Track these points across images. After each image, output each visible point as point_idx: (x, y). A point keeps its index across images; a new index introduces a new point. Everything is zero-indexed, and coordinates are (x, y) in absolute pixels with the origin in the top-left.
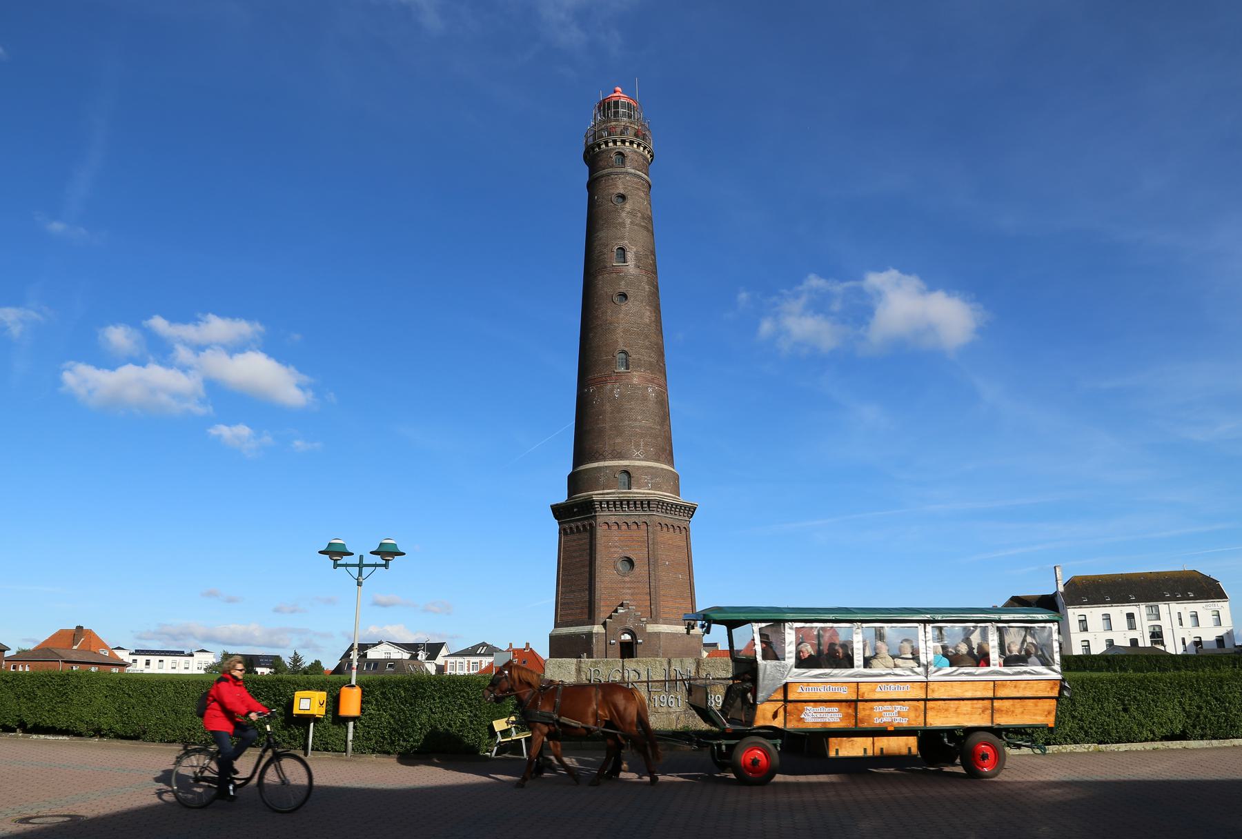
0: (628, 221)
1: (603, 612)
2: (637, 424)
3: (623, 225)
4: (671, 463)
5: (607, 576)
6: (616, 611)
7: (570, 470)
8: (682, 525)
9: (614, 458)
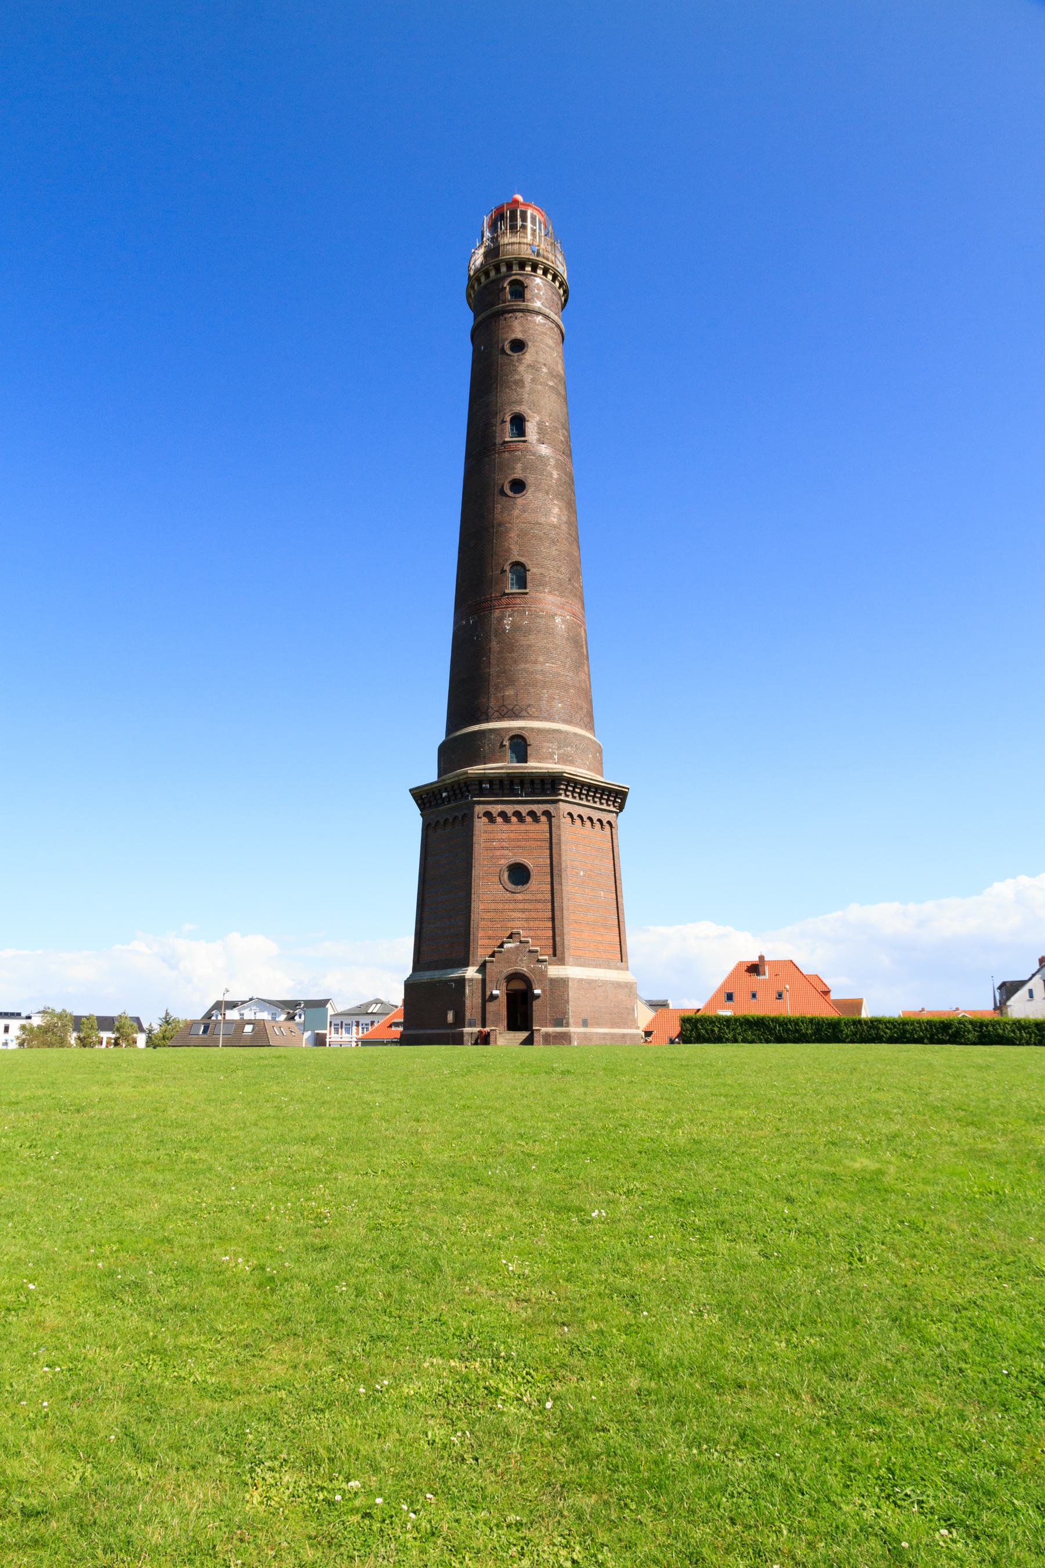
0: (528, 378)
1: (481, 950)
2: (539, 667)
3: (520, 383)
4: (590, 726)
5: (488, 891)
6: (501, 946)
8: (606, 817)
9: (502, 717)
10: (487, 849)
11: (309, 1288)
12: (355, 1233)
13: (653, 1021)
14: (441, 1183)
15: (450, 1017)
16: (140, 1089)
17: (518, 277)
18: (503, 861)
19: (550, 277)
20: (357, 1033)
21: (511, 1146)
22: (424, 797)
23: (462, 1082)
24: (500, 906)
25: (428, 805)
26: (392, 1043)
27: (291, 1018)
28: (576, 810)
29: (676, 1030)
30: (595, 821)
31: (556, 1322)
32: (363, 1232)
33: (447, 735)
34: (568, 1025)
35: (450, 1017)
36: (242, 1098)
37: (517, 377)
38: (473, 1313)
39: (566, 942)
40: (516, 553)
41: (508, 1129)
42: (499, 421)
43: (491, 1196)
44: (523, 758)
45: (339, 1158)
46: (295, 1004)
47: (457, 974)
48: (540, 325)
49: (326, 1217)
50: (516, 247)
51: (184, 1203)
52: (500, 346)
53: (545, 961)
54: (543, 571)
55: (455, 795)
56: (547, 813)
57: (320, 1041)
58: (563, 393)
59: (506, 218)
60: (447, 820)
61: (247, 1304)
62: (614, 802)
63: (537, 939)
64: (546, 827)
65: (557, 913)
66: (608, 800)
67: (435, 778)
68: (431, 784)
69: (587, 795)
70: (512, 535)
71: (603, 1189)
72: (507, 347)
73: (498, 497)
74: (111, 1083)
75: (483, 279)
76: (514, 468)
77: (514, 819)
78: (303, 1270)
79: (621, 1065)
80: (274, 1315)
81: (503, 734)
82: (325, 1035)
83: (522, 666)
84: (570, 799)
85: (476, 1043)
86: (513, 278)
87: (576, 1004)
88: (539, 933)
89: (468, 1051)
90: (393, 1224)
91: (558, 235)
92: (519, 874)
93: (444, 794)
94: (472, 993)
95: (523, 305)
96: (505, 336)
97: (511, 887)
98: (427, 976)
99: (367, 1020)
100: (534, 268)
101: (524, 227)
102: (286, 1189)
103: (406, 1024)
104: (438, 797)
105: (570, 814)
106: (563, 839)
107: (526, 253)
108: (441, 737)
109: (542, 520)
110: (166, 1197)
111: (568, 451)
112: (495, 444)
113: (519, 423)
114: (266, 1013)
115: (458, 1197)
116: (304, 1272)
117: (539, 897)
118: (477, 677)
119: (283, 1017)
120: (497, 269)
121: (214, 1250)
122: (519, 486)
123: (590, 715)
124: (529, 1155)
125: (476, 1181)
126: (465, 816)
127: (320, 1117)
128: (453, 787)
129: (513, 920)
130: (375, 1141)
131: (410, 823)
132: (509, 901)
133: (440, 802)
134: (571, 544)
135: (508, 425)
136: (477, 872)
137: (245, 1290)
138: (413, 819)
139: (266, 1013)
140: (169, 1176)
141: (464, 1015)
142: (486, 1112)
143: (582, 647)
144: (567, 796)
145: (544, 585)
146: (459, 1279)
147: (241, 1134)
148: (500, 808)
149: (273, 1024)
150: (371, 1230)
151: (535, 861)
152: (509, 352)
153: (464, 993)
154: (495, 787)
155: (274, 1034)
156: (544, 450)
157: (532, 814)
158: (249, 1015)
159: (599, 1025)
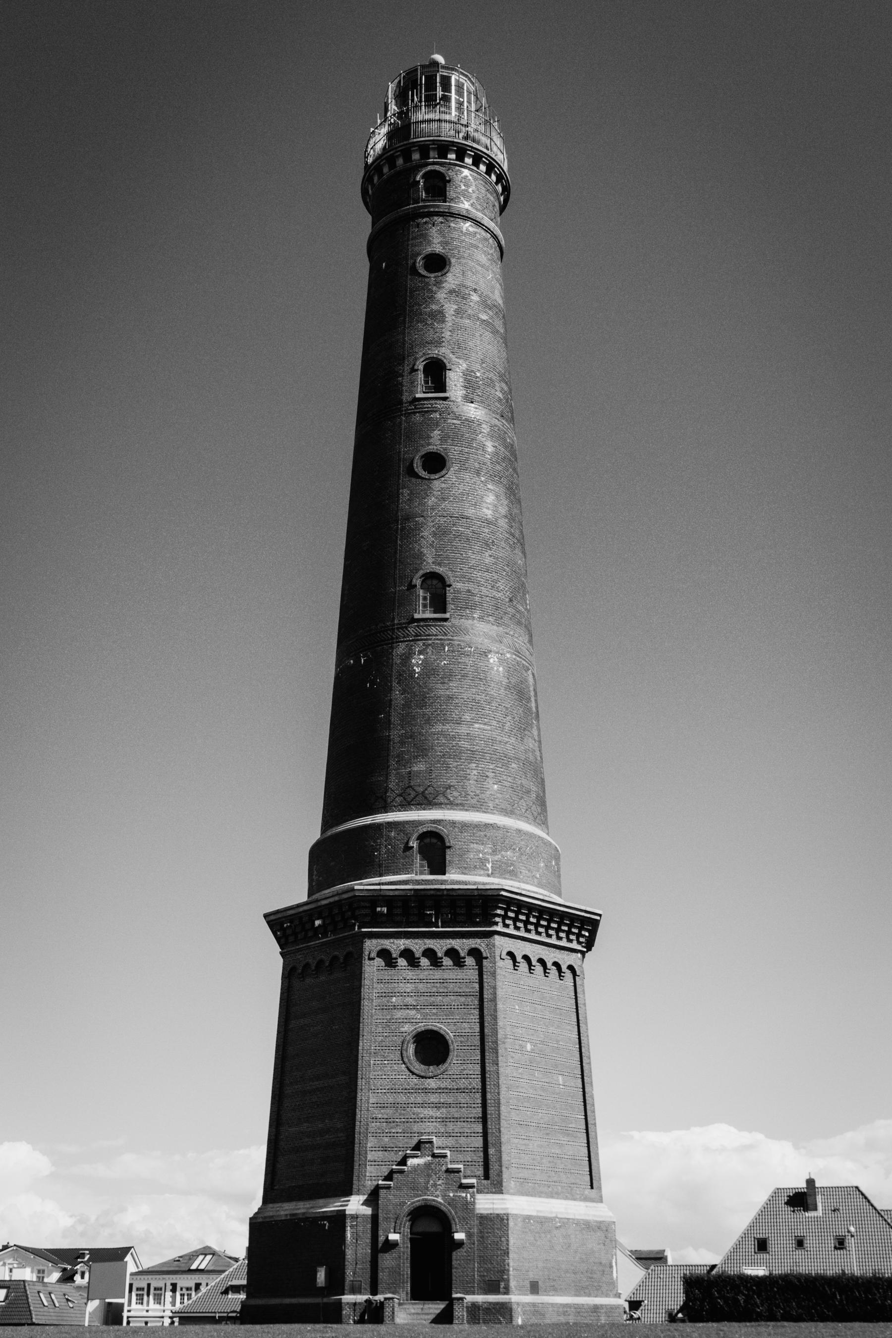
0: (450, 309)
1: (372, 1169)
3: (439, 316)
4: (541, 816)
5: (383, 1075)
6: (403, 1162)
7: (315, 834)
8: (566, 959)
9: (406, 805)
13: (642, 1285)
15: (321, 1276)
17: (437, 168)
19: (483, 168)
22: (285, 925)
24: (402, 1098)
26: (226, 1319)
27: (68, 1278)
28: (521, 949)
29: (676, 1298)
30: (549, 965)
33: (323, 831)
34: (507, 1291)
35: (321, 1276)
37: (434, 307)
39: (505, 1157)
42: (407, 368)
44: (438, 866)
47: (333, 1207)
48: (468, 234)
50: (435, 125)
52: (410, 262)
53: (472, 1187)
54: (471, 586)
56: (475, 953)
59: (422, 84)
60: (321, 962)
62: (579, 935)
63: (458, 1148)
64: (473, 974)
65: (490, 1110)
66: (569, 933)
68: (298, 906)
70: (425, 534)
72: (420, 263)
73: (404, 479)
75: (386, 170)
76: (429, 437)
77: (425, 962)
81: (409, 829)
82: (122, 1305)
83: (439, 727)
84: (511, 931)
85: (361, 1321)
86: (429, 168)
87: (521, 1259)
88: (462, 1140)
91: (497, 108)
92: (432, 1048)
93: (318, 923)
94: (356, 1237)
95: (443, 206)
97: (418, 1067)
98: (285, 1209)
100: (461, 157)
101: (446, 99)
104: (308, 926)
105: (511, 954)
106: (500, 993)
107: (447, 133)
108: (314, 834)
109: (470, 512)
111: (509, 413)
112: (401, 402)
113: (437, 372)
114: (28, 1270)
117: (463, 1083)
119: (56, 1276)
120: (406, 154)
122: (436, 463)
123: (541, 802)
126: (349, 955)
131: (263, 968)
132: (417, 1090)
133: (310, 934)
134: (512, 547)
135: (421, 376)
136: (367, 1043)
138: (267, 963)
139: (28, 1270)
141: (343, 1273)
143: (529, 700)
144: (507, 926)
145: (473, 607)
148: (402, 944)
151: (457, 1028)
152: (423, 272)
156: (473, 411)
157: (452, 953)
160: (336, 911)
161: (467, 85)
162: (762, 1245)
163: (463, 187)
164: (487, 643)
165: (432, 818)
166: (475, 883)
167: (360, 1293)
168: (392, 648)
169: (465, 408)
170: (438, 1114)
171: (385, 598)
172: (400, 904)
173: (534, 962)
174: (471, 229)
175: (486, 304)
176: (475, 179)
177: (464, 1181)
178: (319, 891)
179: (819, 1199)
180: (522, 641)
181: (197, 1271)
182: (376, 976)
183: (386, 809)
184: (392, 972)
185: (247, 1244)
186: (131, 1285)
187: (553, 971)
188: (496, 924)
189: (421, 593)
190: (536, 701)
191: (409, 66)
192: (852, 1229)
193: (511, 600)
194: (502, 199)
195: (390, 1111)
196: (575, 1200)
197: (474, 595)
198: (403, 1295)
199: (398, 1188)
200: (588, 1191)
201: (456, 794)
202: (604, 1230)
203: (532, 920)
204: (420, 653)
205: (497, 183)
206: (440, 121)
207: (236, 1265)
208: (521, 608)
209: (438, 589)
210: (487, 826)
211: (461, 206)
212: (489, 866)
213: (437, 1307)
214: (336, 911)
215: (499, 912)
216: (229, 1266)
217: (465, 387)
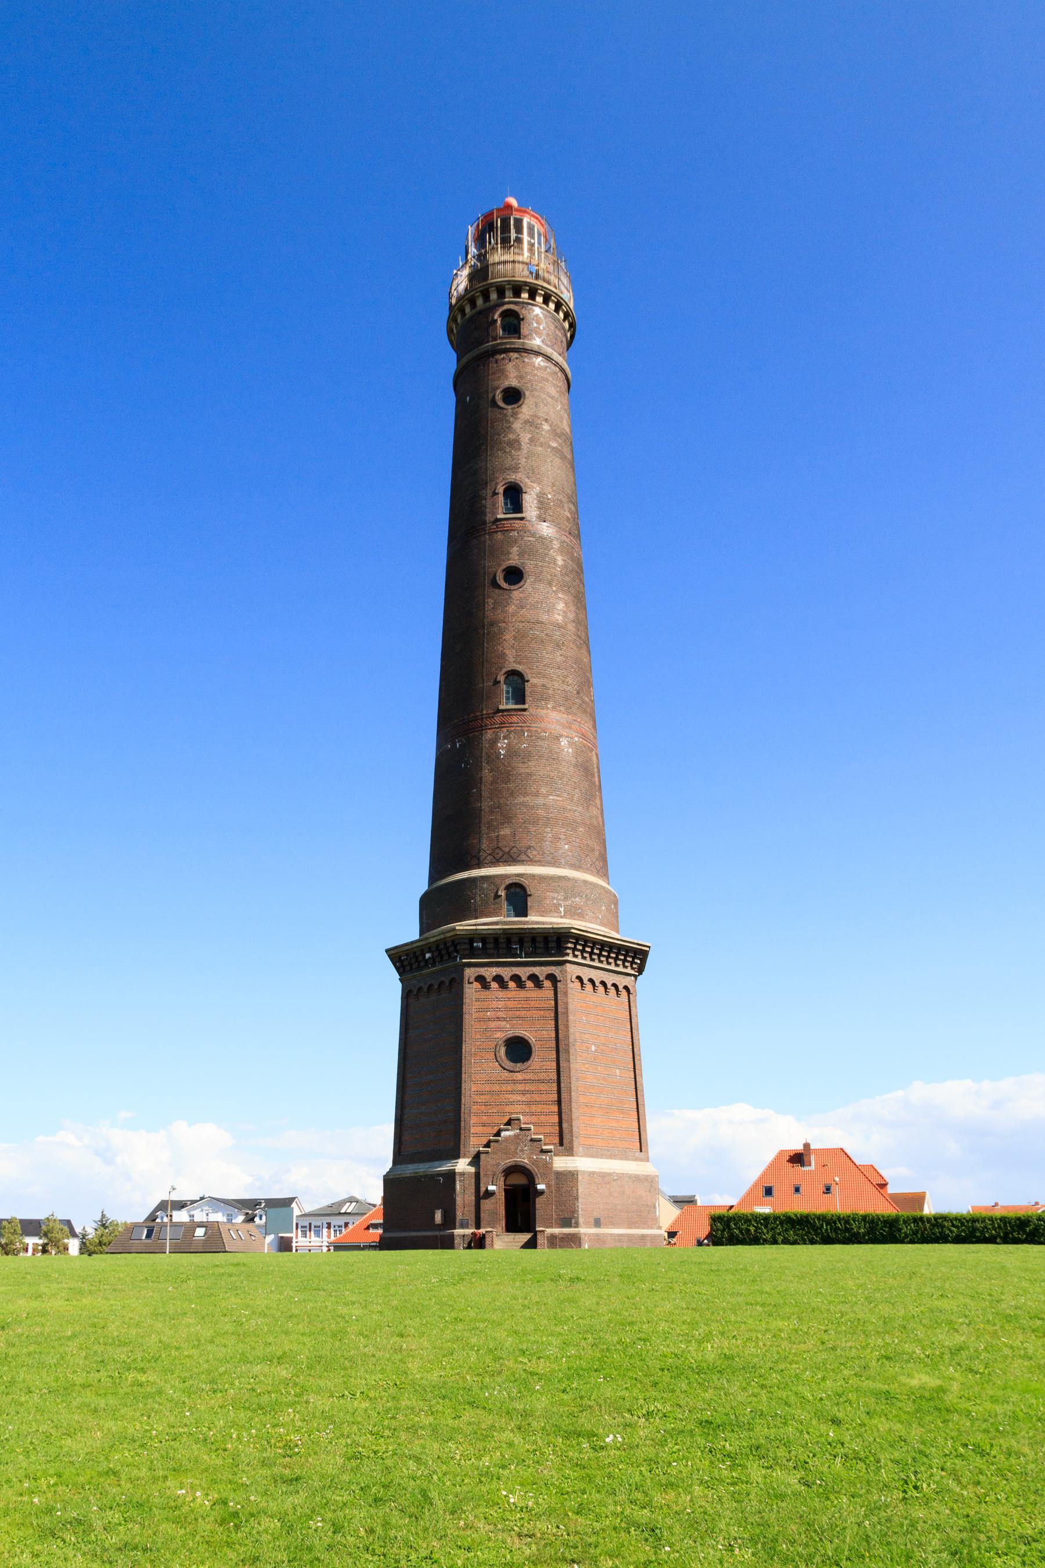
0: (525, 437)
1: (474, 1138)
2: (540, 801)
3: (515, 444)
5: (481, 1071)
6: (498, 1134)
8: (622, 981)
9: (496, 862)
10: (480, 1020)
11: (279, 1524)
12: (332, 1463)
14: (431, 1406)
15: (438, 1217)
16: (75, 1303)
18: (499, 1035)
19: (552, 306)
20: (329, 1237)
21: (511, 1364)
23: (453, 1291)
24: (496, 1088)
25: (408, 968)
27: (250, 1219)
28: (586, 974)
29: (704, 1229)
30: (609, 986)
31: (564, 1559)
32: (340, 1461)
34: (577, 1225)
35: (438, 1217)
36: (195, 1312)
37: (511, 436)
38: (469, 1549)
39: (575, 1129)
40: (512, 660)
41: (507, 1344)
42: (489, 492)
43: (488, 1420)
44: (522, 910)
45: (311, 1379)
46: (254, 1204)
47: (445, 1167)
48: (539, 368)
49: (297, 1446)
50: (510, 266)
51: (131, 1430)
52: (490, 396)
53: (550, 1151)
54: (545, 681)
55: (441, 956)
56: (551, 977)
57: (285, 1245)
58: (569, 457)
59: (497, 228)
61: (207, 1543)
62: (632, 963)
63: (540, 1124)
64: (550, 994)
65: (564, 1095)
66: (624, 961)
67: (416, 936)
68: (412, 943)
69: (600, 955)
70: (507, 637)
71: (618, 1411)
72: (499, 397)
73: (489, 590)
74: (40, 1296)
75: (468, 309)
76: (509, 553)
77: (512, 985)
78: (271, 1504)
79: (640, 1271)
80: (239, 1554)
81: (498, 882)
83: (521, 799)
84: (579, 960)
85: (469, 1247)
86: (506, 307)
87: (586, 1202)
88: (543, 1118)
89: (459, 1257)
90: (375, 1453)
92: (518, 1050)
93: (428, 956)
95: (517, 343)
96: (496, 383)
98: (409, 1170)
99: (340, 1221)
100: (532, 295)
101: (519, 240)
102: (250, 1414)
103: (386, 1226)
104: (420, 958)
105: (579, 978)
106: (571, 1007)
107: (522, 274)
108: (422, 885)
109: (544, 618)
110: (110, 1424)
112: (485, 523)
113: (514, 495)
114: (220, 1214)
115: (450, 1421)
116: (273, 1506)
118: (466, 812)
119: (241, 1218)
120: (486, 296)
121: (168, 1483)
122: (515, 575)
123: (603, 858)
124: (532, 1374)
125: (471, 1404)
126: (453, 980)
127: (287, 1333)
128: (438, 946)
129: (512, 1103)
130: (351, 1360)
132: (507, 1082)
133: (422, 964)
134: (579, 648)
135: (501, 498)
136: (465, 1048)
137: (205, 1527)
138: (390, 986)
139: (220, 1214)
140: (112, 1401)
141: (455, 1214)
142: (482, 1326)
143: (593, 775)
145: (545, 698)
146: (453, 1513)
147: (195, 1352)
148: (495, 971)
149: (229, 1226)
150: (349, 1459)
152: (501, 404)
153: (454, 1189)
154: (488, 946)
155: (230, 1238)
156: (546, 529)
157: (533, 978)
158: (200, 1216)
159: (614, 1225)
160: (442, 946)
161: (537, 227)
162: (769, 1191)
163: (535, 325)
164: (558, 729)
165: (516, 872)
166: (551, 923)
167: (468, 1228)
168: (482, 734)
169: (539, 527)
170: (524, 1099)
171: (474, 692)
172: (492, 940)
173: (597, 984)
174: (542, 364)
175: (555, 433)
176: (545, 317)
177: (544, 1147)
178: (429, 931)
179: (813, 1157)
180: (587, 727)
181: (345, 1213)
182: (475, 996)
183: (479, 865)
184: (487, 992)
185: (382, 1194)
186: (297, 1224)
187: (612, 990)
188: (568, 954)
189: (504, 687)
190: (599, 776)
191: (486, 210)
192: (837, 1179)
193: (578, 693)
194: (569, 335)
195: (487, 1098)
196: (628, 1160)
197: (548, 689)
198: (500, 1229)
199: (494, 1153)
200: (638, 1154)
201: (535, 852)
202: (650, 1182)
203: (596, 951)
204: (505, 738)
205: (564, 320)
206: (514, 262)
207: (374, 1209)
208: (586, 699)
209: (518, 683)
210: (560, 878)
211: (534, 342)
212: (562, 909)
213: (526, 1237)
214: (442, 946)
215: (570, 945)
216: (370, 1210)
217: (539, 508)
